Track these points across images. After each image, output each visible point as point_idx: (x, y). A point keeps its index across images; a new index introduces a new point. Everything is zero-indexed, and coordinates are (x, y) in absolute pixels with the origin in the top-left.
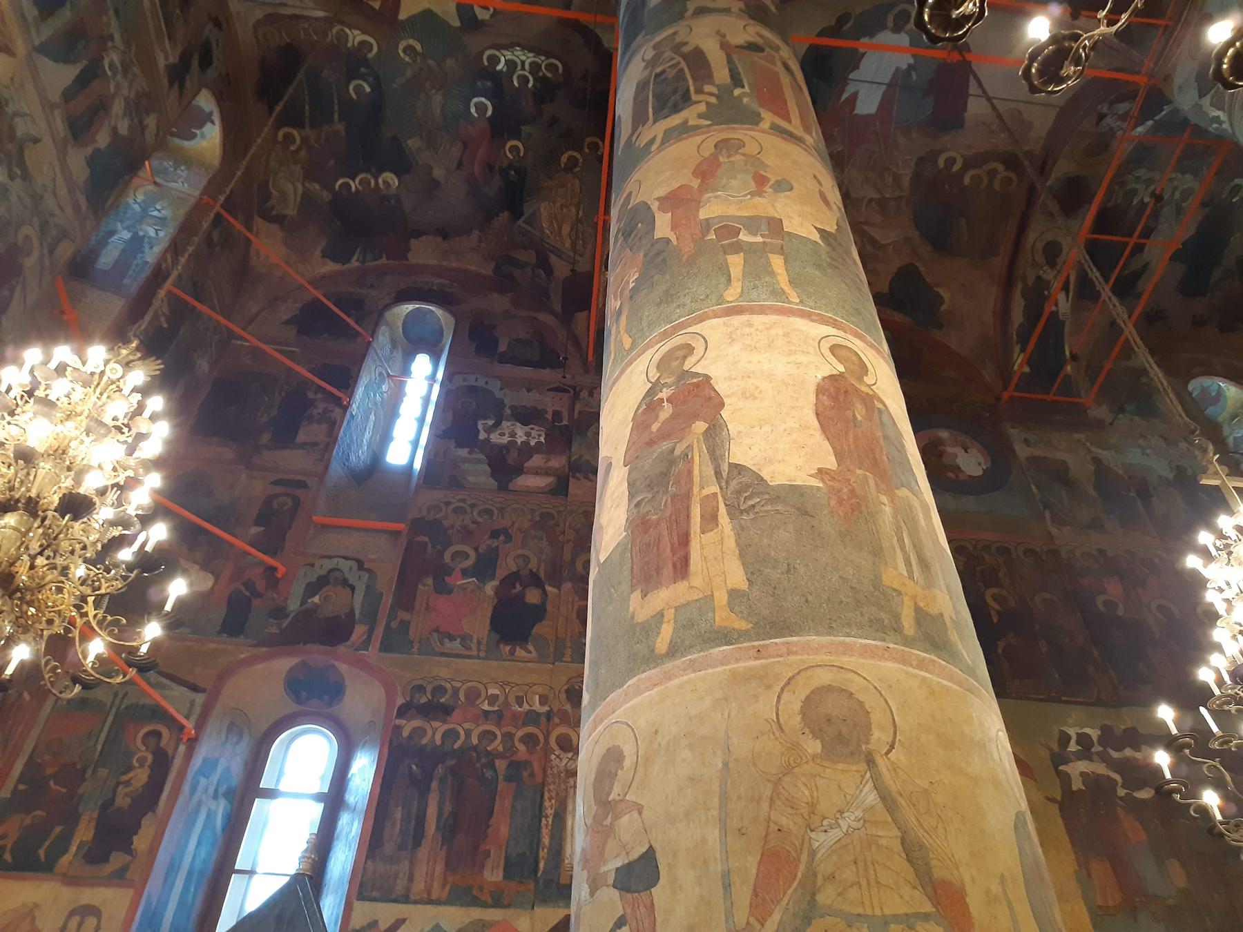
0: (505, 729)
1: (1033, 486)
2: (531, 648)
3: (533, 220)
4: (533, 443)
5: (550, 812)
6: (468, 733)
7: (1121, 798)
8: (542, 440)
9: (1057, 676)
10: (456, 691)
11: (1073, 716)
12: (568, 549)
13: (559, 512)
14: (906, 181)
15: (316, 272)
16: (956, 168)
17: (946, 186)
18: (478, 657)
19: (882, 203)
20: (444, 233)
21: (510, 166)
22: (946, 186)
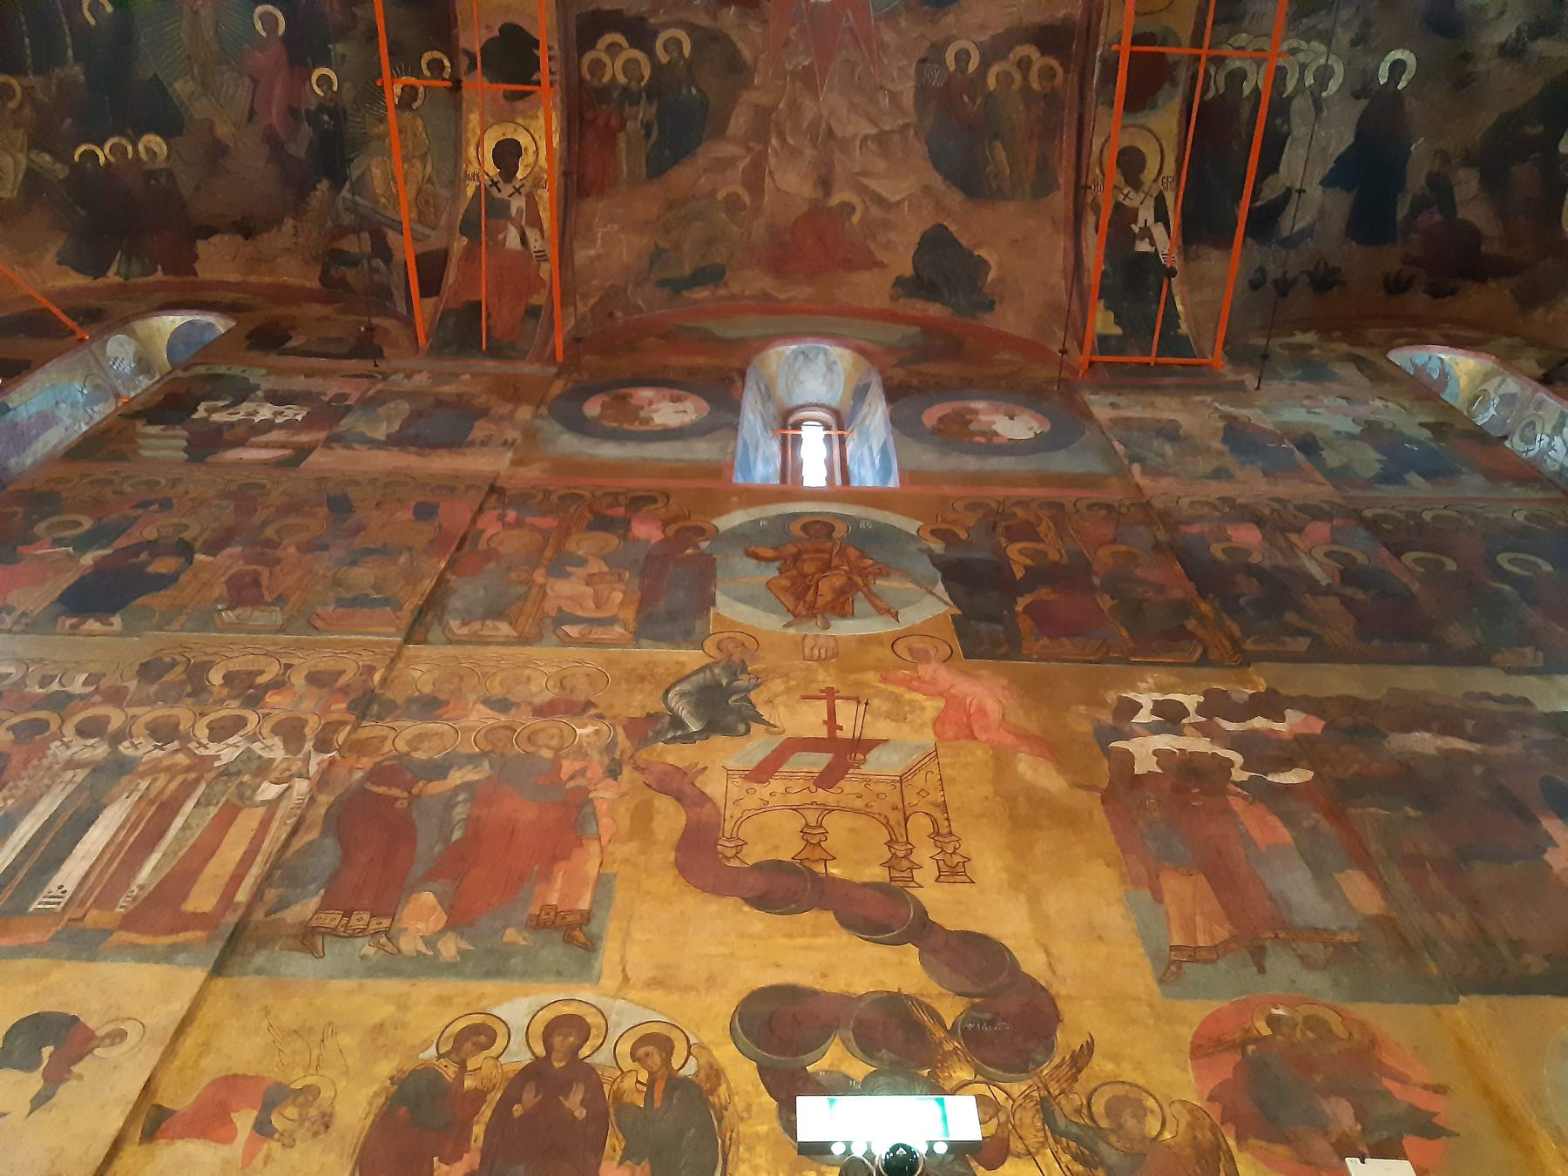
1: (1116, 444)
3: (360, 186)
4: (279, 420)
7: (1240, 784)
8: (299, 418)
9: (1125, 633)
11: (1150, 680)
14: (908, 99)
15: (50, 284)
16: (973, 66)
17: (966, 98)
18: (10, 631)
19: (882, 139)
20: (247, 229)
21: (322, 108)
22: (966, 98)
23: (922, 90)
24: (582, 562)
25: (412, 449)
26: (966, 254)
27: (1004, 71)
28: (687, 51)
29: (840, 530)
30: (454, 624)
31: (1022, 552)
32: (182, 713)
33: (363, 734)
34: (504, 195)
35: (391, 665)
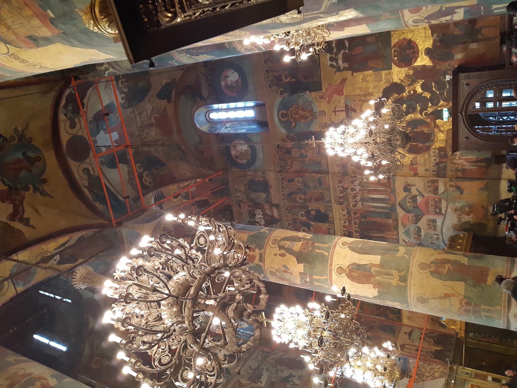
0: (353, 219)
2: (329, 213)
5: (373, 209)
6: (355, 228)
7: (349, 52)
10: (344, 231)
12: (296, 204)
13: (284, 206)
14: (131, 109)
19: (140, 114)
23: (129, 107)
24: (302, 154)
25: (269, 188)
26: (163, 88)
27: (124, 87)
28: (139, 164)
29: (281, 112)
30: (323, 168)
31: (286, 78)
32: (350, 197)
33: (351, 173)
34: (184, 194)
35: (336, 174)
